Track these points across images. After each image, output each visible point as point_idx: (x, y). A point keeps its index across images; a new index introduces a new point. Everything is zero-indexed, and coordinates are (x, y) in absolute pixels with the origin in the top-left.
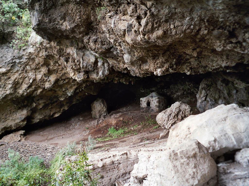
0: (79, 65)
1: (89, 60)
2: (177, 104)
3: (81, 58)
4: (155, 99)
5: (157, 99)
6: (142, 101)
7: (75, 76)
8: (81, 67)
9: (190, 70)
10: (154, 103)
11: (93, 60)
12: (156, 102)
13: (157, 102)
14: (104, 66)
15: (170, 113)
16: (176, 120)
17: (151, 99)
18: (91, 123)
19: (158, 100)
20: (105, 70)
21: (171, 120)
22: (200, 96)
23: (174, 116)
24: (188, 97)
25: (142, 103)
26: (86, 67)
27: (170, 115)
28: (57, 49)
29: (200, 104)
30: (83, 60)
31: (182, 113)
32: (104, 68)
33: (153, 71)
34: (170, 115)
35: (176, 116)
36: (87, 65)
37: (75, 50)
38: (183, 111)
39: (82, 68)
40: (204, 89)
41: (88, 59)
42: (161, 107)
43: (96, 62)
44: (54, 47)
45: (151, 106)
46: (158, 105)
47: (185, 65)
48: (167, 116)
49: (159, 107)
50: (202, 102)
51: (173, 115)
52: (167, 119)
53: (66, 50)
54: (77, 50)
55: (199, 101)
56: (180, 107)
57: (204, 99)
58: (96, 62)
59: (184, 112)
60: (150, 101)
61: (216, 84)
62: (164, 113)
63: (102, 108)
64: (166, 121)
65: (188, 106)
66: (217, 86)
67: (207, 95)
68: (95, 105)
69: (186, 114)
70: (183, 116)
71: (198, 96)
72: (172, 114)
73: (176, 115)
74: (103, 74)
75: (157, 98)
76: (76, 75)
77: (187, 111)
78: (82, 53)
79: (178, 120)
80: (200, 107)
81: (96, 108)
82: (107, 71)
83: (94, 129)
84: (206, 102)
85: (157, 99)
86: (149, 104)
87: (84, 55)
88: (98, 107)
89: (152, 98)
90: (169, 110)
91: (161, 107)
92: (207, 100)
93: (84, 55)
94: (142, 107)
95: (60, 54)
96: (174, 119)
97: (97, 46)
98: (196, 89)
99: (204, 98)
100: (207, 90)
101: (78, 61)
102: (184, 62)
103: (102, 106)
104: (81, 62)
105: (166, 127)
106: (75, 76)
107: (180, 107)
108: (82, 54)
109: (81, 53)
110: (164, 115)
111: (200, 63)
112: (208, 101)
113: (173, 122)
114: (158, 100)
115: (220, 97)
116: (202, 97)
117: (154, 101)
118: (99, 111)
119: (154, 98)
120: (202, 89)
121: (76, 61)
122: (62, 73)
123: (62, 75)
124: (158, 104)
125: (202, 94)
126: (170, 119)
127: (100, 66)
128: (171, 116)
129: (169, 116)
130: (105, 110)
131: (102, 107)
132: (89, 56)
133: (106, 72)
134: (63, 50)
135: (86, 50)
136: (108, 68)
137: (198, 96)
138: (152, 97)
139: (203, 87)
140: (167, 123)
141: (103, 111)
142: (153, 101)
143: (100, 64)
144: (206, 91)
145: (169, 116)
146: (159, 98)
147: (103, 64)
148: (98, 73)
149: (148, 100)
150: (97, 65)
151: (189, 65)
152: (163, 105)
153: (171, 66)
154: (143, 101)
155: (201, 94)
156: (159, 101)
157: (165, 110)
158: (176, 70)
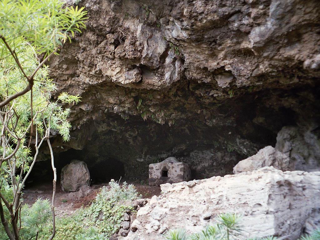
0: (141, 51)
1: (156, 48)
3: (146, 41)
4: (178, 165)
5: (181, 165)
6: (152, 168)
7: (120, 75)
8: (144, 56)
10: (176, 171)
11: (161, 49)
12: (178, 170)
13: (181, 170)
14: (174, 65)
17: (170, 165)
19: (183, 166)
20: (175, 73)
24: (222, 169)
25: (153, 172)
26: (150, 58)
28: (109, 17)
30: (148, 44)
32: (175, 69)
36: (153, 56)
37: (141, 25)
39: (144, 58)
41: (155, 46)
42: (186, 178)
43: (164, 56)
44: (106, 12)
45: (169, 176)
46: (182, 174)
53: (123, 21)
54: (144, 24)
58: (164, 56)
60: (167, 168)
61: (302, 136)
66: (303, 139)
74: (171, 78)
76: (122, 74)
78: (150, 34)
81: (75, 174)
82: (178, 75)
83: (77, 203)
85: (181, 165)
87: (151, 37)
89: (172, 164)
93: (151, 37)
94: (152, 178)
95: (112, 26)
97: (209, 7)
101: (140, 45)
103: (85, 170)
104: (145, 48)
106: (120, 75)
108: (149, 33)
109: (148, 32)
114: (183, 166)
115: (310, 155)
121: (138, 43)
122: (64, 85)
123: (65, 89)
124: (182, 173)
127: (169, 64)
131: (84, 173)
132: (156, 42)
133: (176, 77)
134: (118, 22)
135: (157, 30)
136: (179, 69)
141: (83, 180)
142: (173, 167)
143: (168, 60)
147: (173, 61)
148: (162, 75)
149: (165, 168)
150: (164, 61)
154: (155, 168)
156: (184, 168)
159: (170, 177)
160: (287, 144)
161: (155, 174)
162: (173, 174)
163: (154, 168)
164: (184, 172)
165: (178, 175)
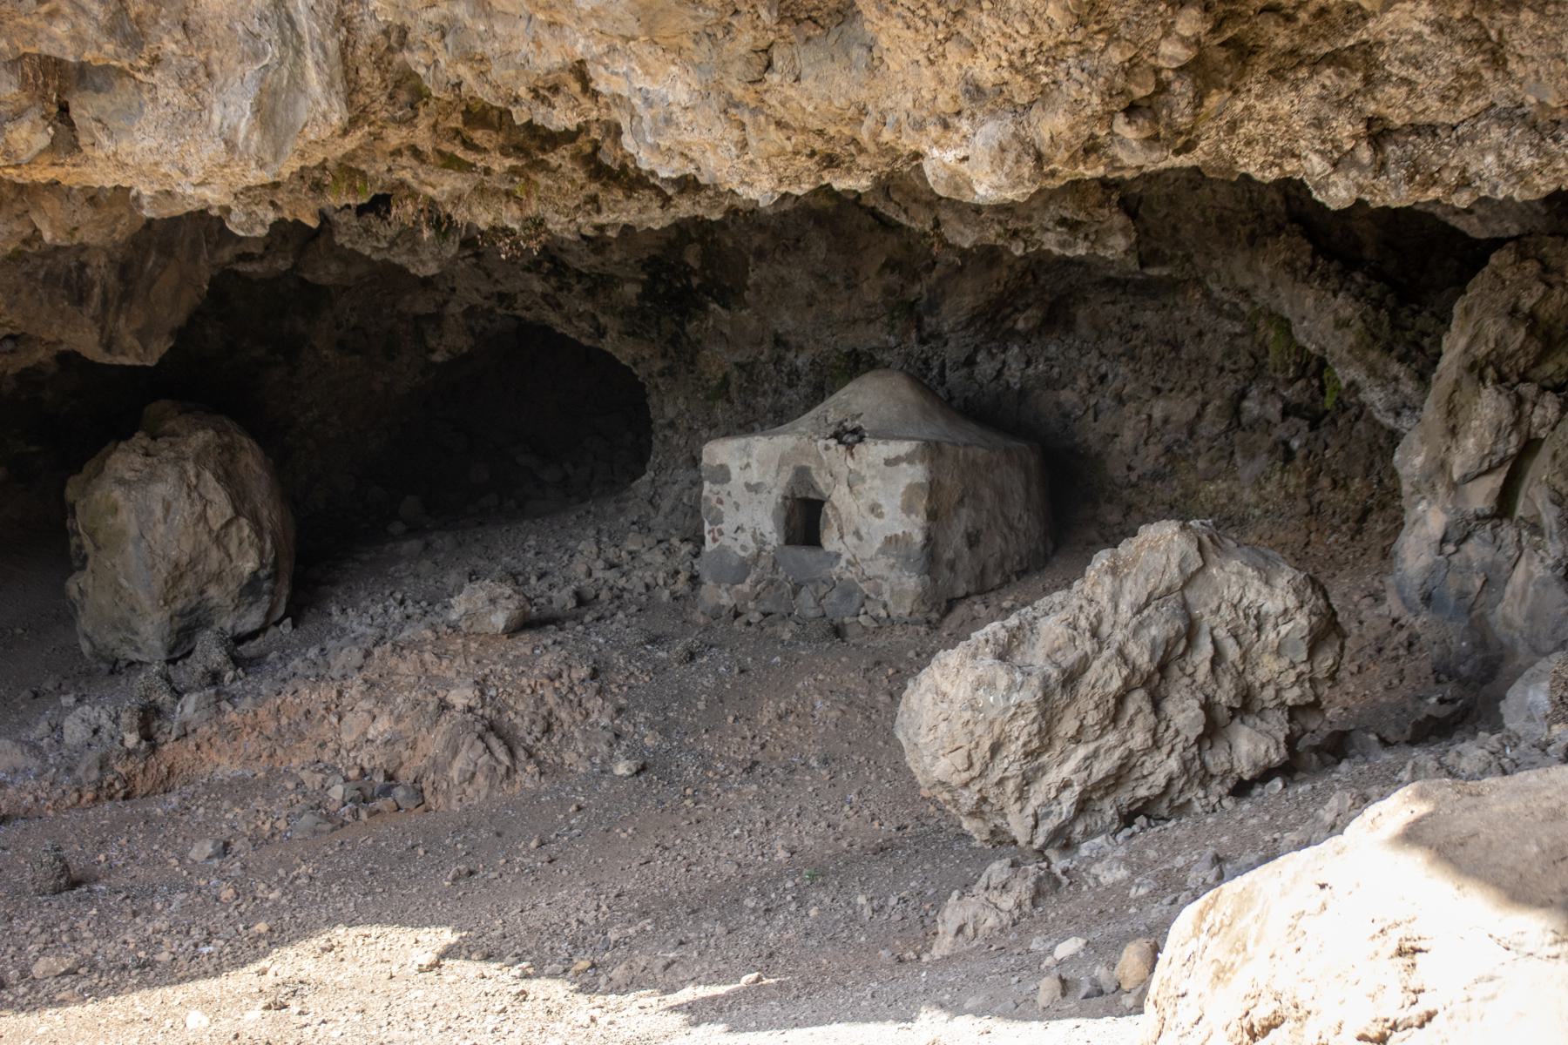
2: (1160, 546)
4: (888, 462)
5: (909, 459)
6: (722, 475)
9: (1365, 154)
10: (875, 509)
12: (892, 505)
13: (908, 508)
15: (1070, 658)
16: (1139, 739)
18: (57, 728)
21: (1077, 739)
22: (1443, 466)
23: (1121, 700)
27: (1071, 678)
29: (1426, 559)
31: (1217, 659)
33: (908, 143)
34: (1071, 678)
35: (1138, 699)
38: (1221, 633)
40: (1501, 379)
42: (952, 566)
46: (918, 538)
47: (1311, 90)
48: (1028, 695)
49: (931, 557)
50: (1457, 535)
51: (1106, 676)
52: (1022, 730)
55: (1429, 519)
56: (1188, 581)
57: (1481, 495)
59: (1232, 652)
60: (822, 481)
62: (1003, 655)
63: (219, 539)
64: (1014, 749)
65: (1285, 577)
67: (1530, 447)
68: (118, 494)
69: (1262, 674)
70: (1225, 694)
71: (1411, 460)
72: (1090, 676)
73: (1146, 683)
75: (905, 447)
77: (1270, 636)
79: (1156, 744)
80: (1427, 599)
84: (1508, 533)
86: (805, 518)
88: (164, 519)
90: (1053, 622)
91: (952, 566)
92: (1520, 511)
94: (722, 551)
96: (1111, 738)
98: (1396, 368)
99: (1495, 482)
100: (1528, 390)
102: (1293, 52)
103: (220, 506)
105: (1018, 827)
107: (1188, 581)
110: (1002, 682)
111: (1497, 59)
112: (1536, 528)
113: (1102, 768)
114: (916, 473)
116: (1466, 479)
117: (879, 493)
118: (177, 576)
119: (875, 452)
120: (1474, 370)
124: (913, 527)
125: (1470, 443)
126: (1068, 726)
128: (1083, 689)
129: (1060, 698)
130: (249, 565)
136: (332, 45)
137: (1418, 461)
138: (849, 436)
139: (1481, 351)
140: (1027, 781)
141: (218, 577)
144: (1520, 401)
145: (1060, 698)
146: (932, 451)
149: (802, 474)
151: (1356, 81)
152: (973, 540)
153: (1139, 93)
155: (1453, 431)
156: (934, 488)
157: (1013, 621)
158: (1188, 148)
159: (838, 556)
160: (1489, 407)
161: (743, 518)
162: (857, 534)
163: (735, 472)
164: (932, 515)
165: (891, 541)
